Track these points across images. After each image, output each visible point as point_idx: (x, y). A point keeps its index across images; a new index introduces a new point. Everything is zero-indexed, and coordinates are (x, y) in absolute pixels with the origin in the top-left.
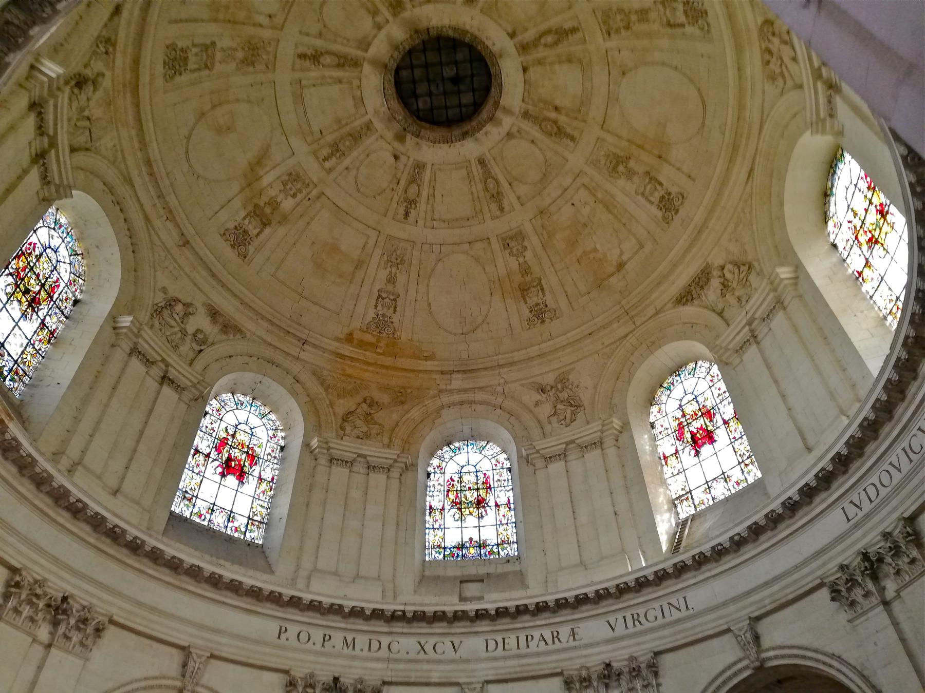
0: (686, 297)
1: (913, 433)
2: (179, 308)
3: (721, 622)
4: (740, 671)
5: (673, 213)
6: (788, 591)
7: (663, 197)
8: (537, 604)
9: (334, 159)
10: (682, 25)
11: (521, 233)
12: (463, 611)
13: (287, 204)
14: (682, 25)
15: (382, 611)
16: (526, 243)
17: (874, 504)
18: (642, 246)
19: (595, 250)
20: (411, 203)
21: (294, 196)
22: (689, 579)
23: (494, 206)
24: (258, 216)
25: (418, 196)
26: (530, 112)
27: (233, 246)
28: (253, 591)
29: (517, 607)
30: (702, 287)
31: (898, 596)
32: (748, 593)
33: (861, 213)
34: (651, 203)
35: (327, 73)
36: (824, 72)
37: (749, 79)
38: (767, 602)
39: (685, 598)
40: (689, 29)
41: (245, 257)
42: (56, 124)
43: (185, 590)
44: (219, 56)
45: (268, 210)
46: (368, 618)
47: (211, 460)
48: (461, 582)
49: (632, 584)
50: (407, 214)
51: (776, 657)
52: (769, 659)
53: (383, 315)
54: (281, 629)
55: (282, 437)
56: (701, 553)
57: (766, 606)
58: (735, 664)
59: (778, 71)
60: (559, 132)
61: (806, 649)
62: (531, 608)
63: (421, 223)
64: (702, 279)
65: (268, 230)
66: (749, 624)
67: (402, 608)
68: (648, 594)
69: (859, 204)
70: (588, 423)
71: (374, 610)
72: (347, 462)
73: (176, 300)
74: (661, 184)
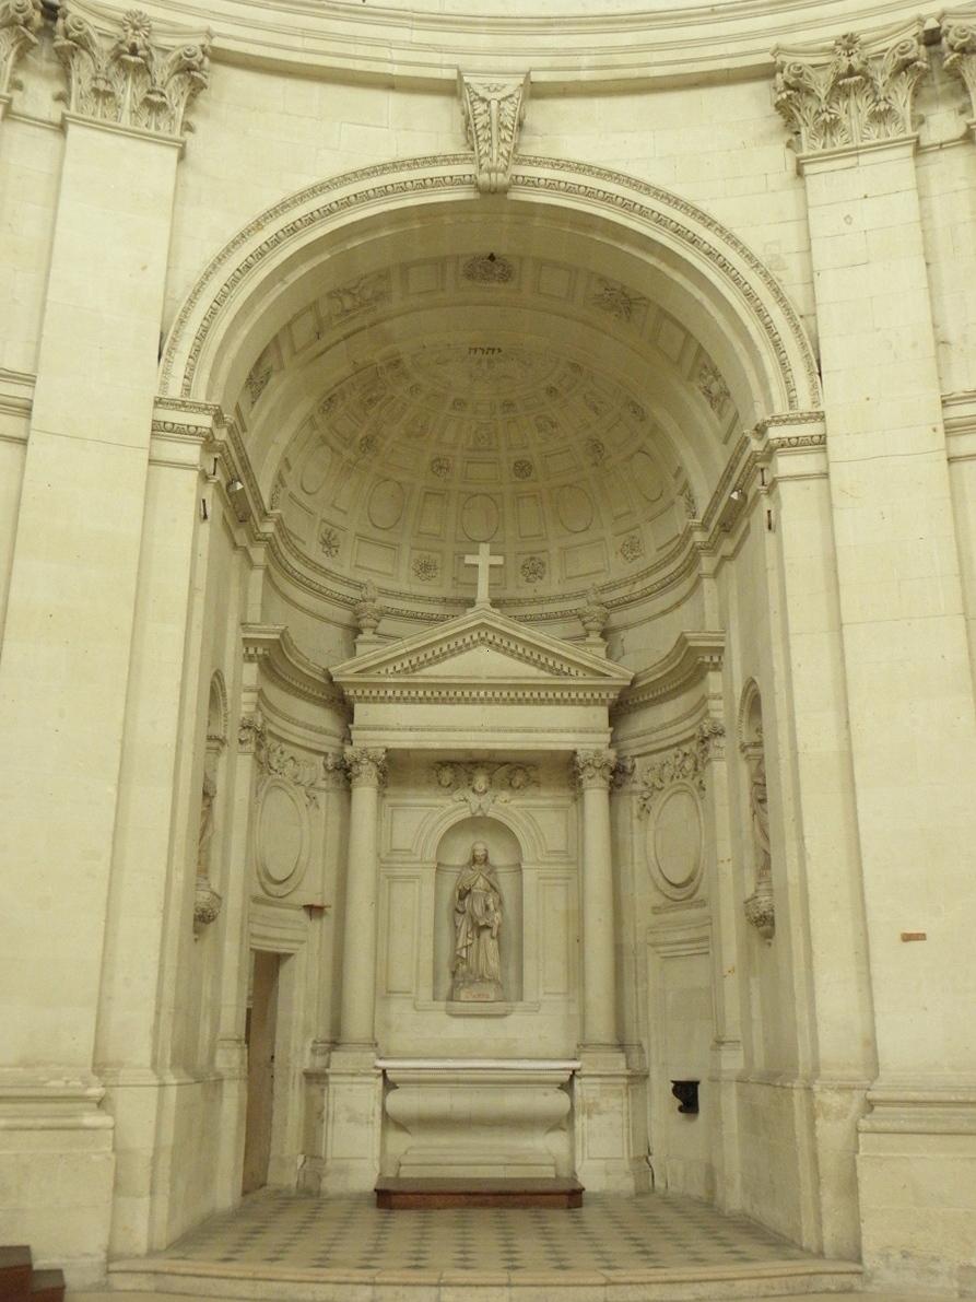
3: (436, 58)
4: (438, 183)
6: (656, 57)
32: (547, 24)
38: (585, 61)
51: (552, 185)
52: (533, 183)
57: (578, 69)
58: (433, 161)
61: (647, 189)
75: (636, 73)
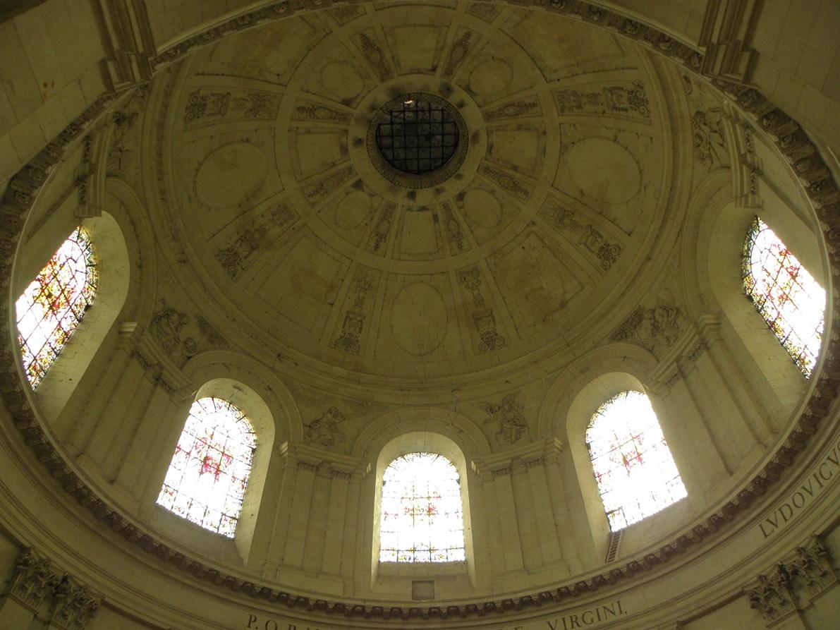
0: (621, 334)
1: (823, 461)
2: (175, 317)
5: (611, 261)
7: (602, 247)
8: (486, 604)
10: (626, 110)
11: (476, 268)
12: (417, 609)
13: (274, 231)
15: (344, 605)
16: (480, 278)
17: (788, 523)
18: (582, 288)
19: (541, 288)
20: (381, 237)
21: (281, 225)
22: (624, 585)
23: (454, 245)
24: (248, 240)
25: (388, 232)
26: (491, 169)
27: (224, 265)
28: (228, 581)
29: (467, 606)
30: (635, 327)
31: (812, 605)
32: (677, 599)
33: (774, 274)
34: (592, 252)
36: (749, 157)
37: (681, 158)
38: (693, 607)
39: (618, 602)
40: (631, 113)
41: (234, 276)
42: (99, 154)
43: (167, 576)
44: (231, 104)
45: (257, 236)
46: (330, 612)
47: (191, 457)
48: (413, 582)
49: (572, 589)
50: (377, 247)
53: (351, 335)
54: (251, 619)
55: (254, 441)
56: (635, 562)
57: (692, 611)
59: (706, 152)
60: (515, 187)
62: (480, 608)
63: (389, 254)
64: (635, 319)
65: (256, 253)
66: (677, 627)
67: (361, 603)
68: (586, 598)
69: (772, 265)
70: (532, 441)
71: (336, 604)
72: (313, 466)
73: (172, 310)
74: (601, 237)
75: (708, 606)
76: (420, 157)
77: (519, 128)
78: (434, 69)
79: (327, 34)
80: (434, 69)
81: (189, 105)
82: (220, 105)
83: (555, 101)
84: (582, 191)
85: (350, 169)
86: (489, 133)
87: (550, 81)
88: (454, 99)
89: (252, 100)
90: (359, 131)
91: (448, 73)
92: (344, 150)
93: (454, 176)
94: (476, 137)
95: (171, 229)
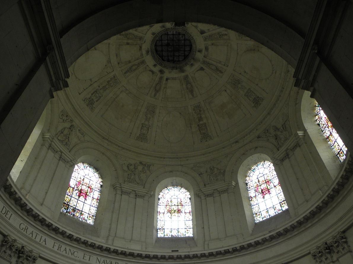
9: (223, 33)
14: (92, 94)
35: (214, 63)
76: (172, 36)
77: (130, 62)
78: (167, 79)
79: (205, 100)
80: (167, 79)
81: (259, 105)
82: (249, 94)
83: (118, 79)
84: (96, 50)
85: (205, 39)
86: (142, 55)
87: (122, 87)
88: (159, 67)
89: (238, 87)
90: (199, 56)
91: (161, 78)
92: (207, 49)
93: (157, 34)
94: (148, 52)
95: (287, 75)
